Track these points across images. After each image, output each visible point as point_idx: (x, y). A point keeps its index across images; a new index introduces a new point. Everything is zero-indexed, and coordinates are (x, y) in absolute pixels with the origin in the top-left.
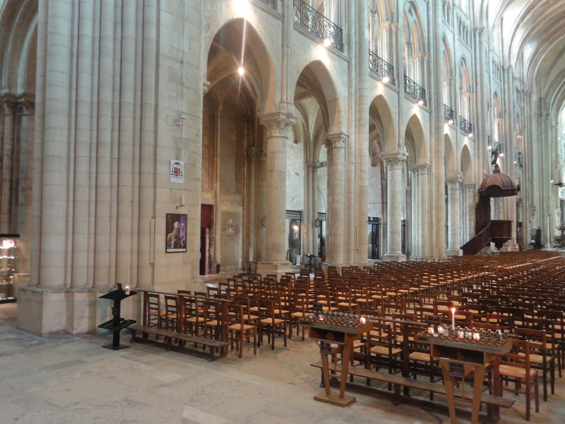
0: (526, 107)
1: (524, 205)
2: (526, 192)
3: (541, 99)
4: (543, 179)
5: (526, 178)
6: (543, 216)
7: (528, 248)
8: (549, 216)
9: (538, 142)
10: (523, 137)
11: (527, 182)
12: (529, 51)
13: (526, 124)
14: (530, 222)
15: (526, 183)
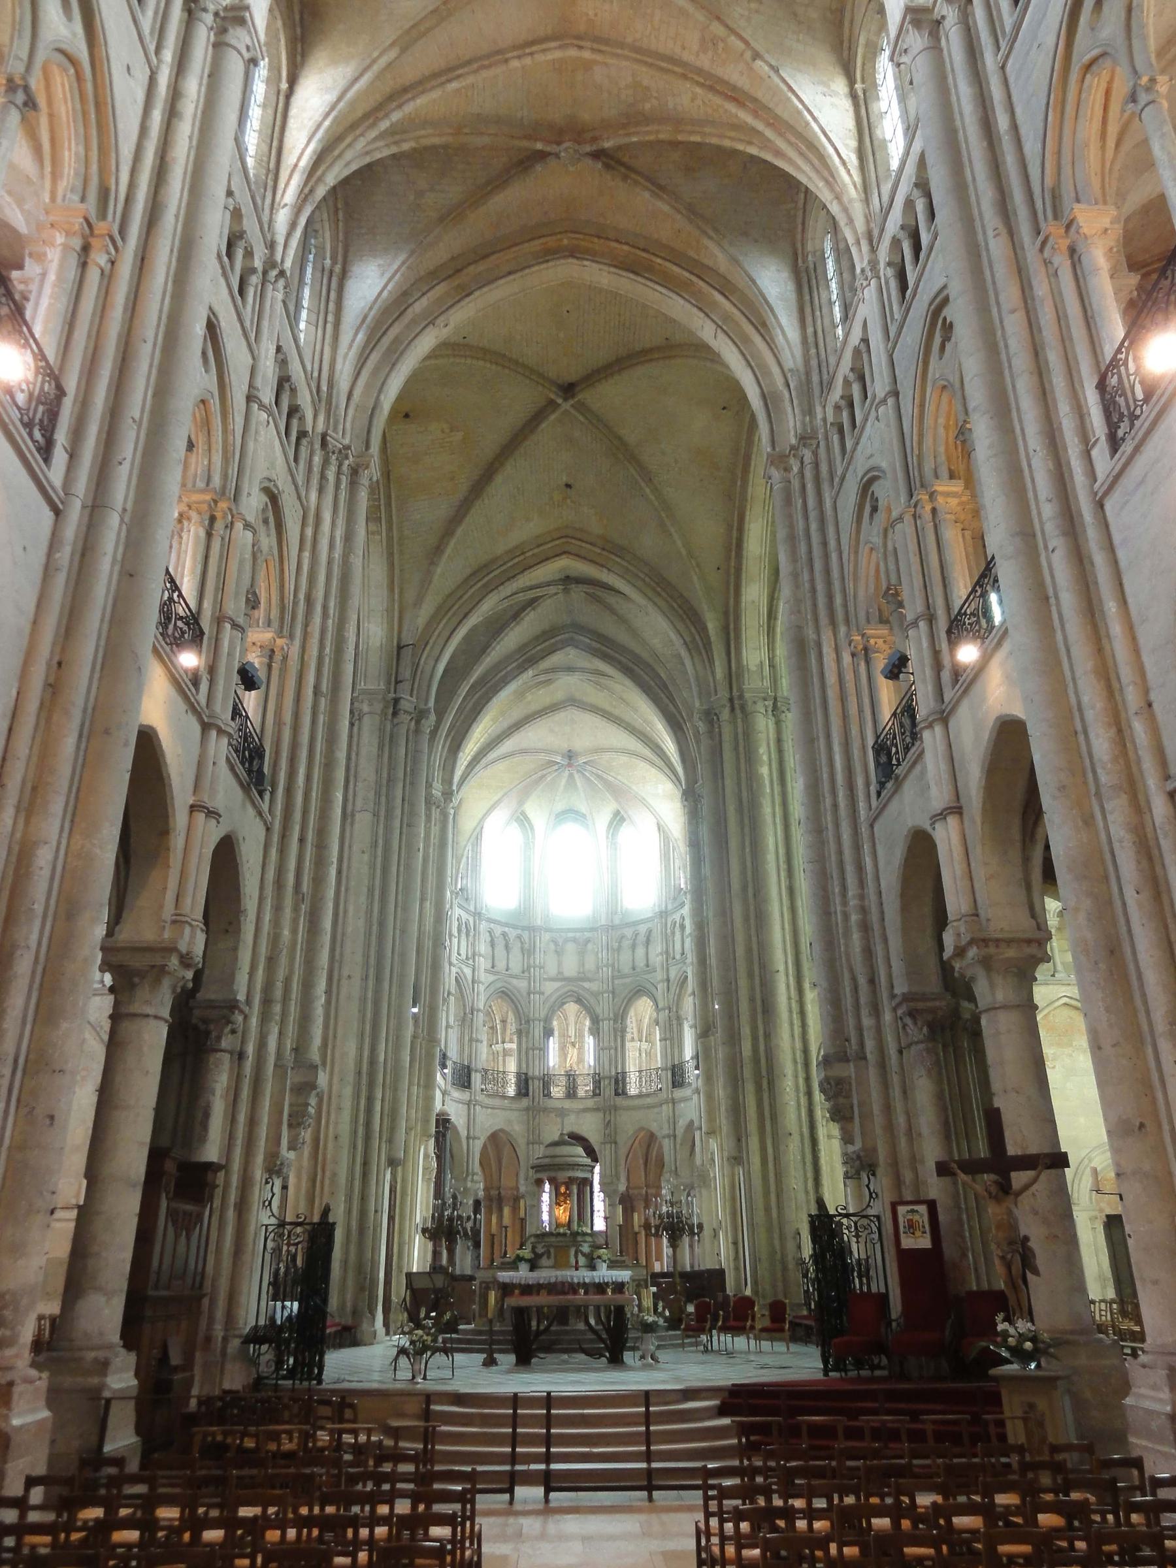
0: (327, 516)
1: (250, 1049)
2: (271, 961)
3: (400, 648)
4: (379, 979)
5: (279, 883)
6: (366, 1164)
7: (234, 1379)
8: (392, 1163)
9: (376, 815)
10: (295, 651)
11: (288, 901)
12: (370, 283)
13: (319, 594)
14: (274, 1168)
15: (278, 909)
